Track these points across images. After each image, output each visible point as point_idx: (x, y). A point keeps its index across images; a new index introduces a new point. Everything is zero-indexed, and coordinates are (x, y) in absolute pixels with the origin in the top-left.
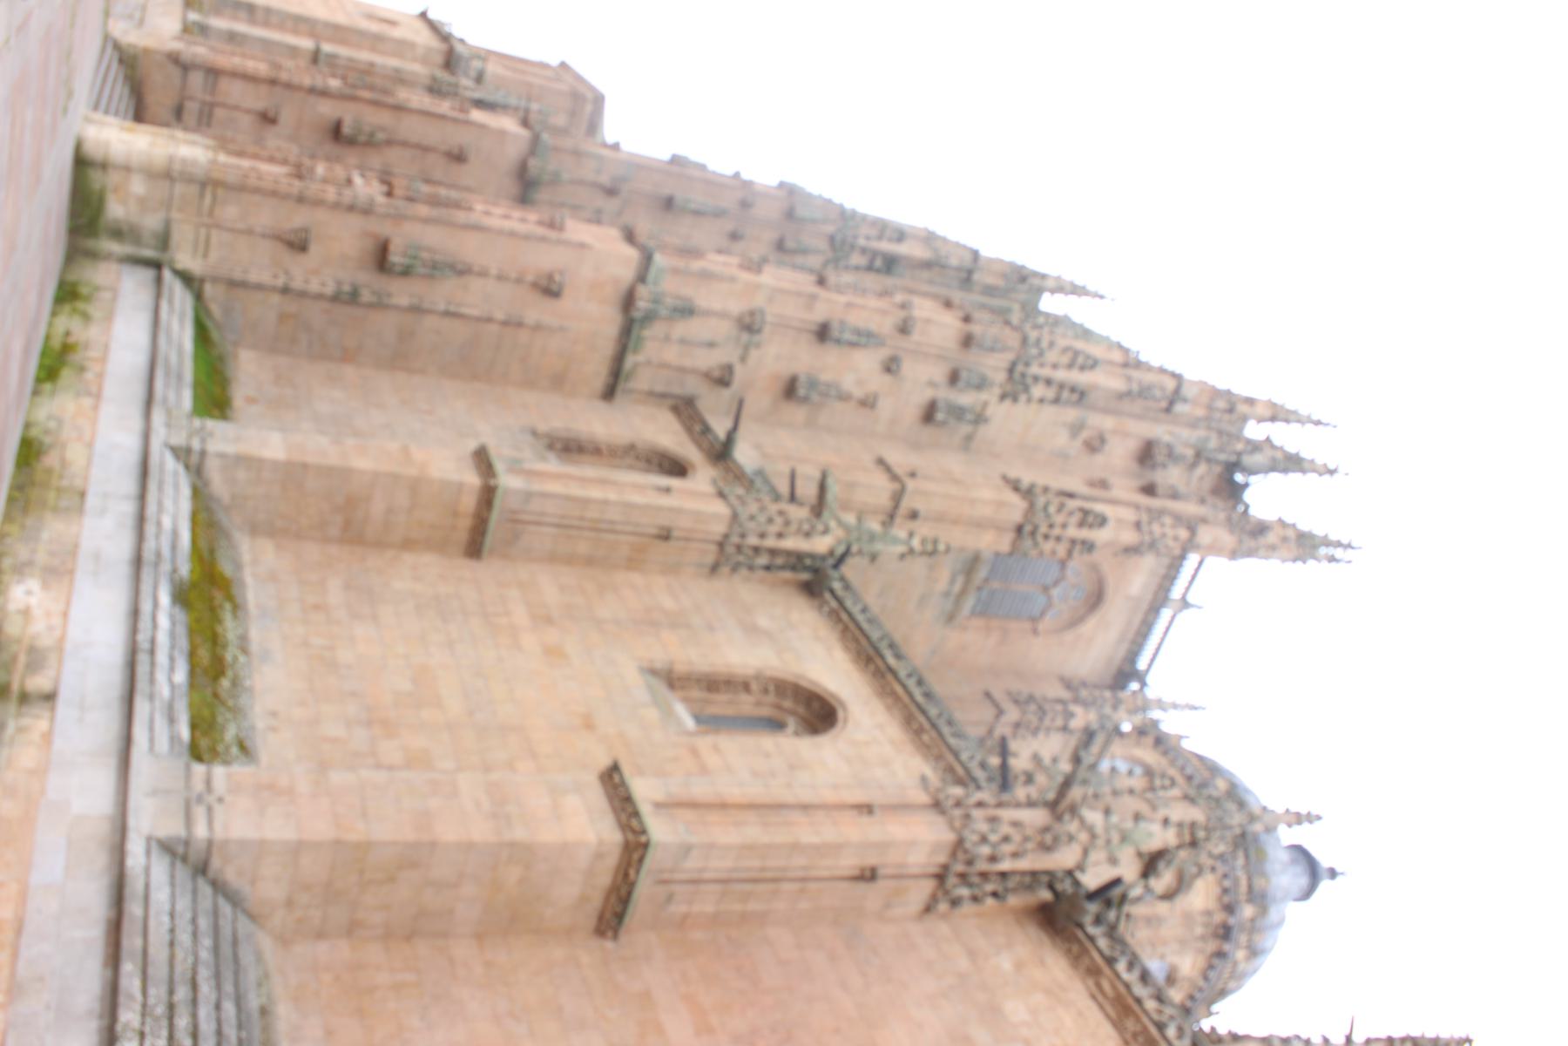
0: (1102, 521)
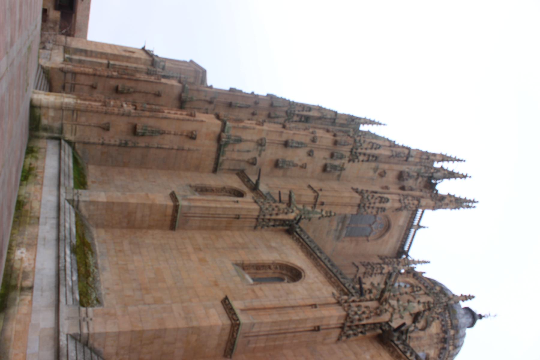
0: (387, 200)
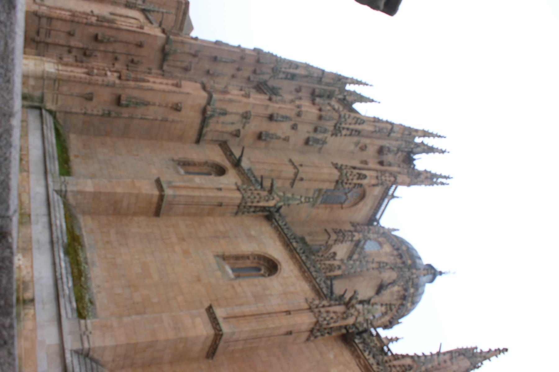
0: (365, 177)
